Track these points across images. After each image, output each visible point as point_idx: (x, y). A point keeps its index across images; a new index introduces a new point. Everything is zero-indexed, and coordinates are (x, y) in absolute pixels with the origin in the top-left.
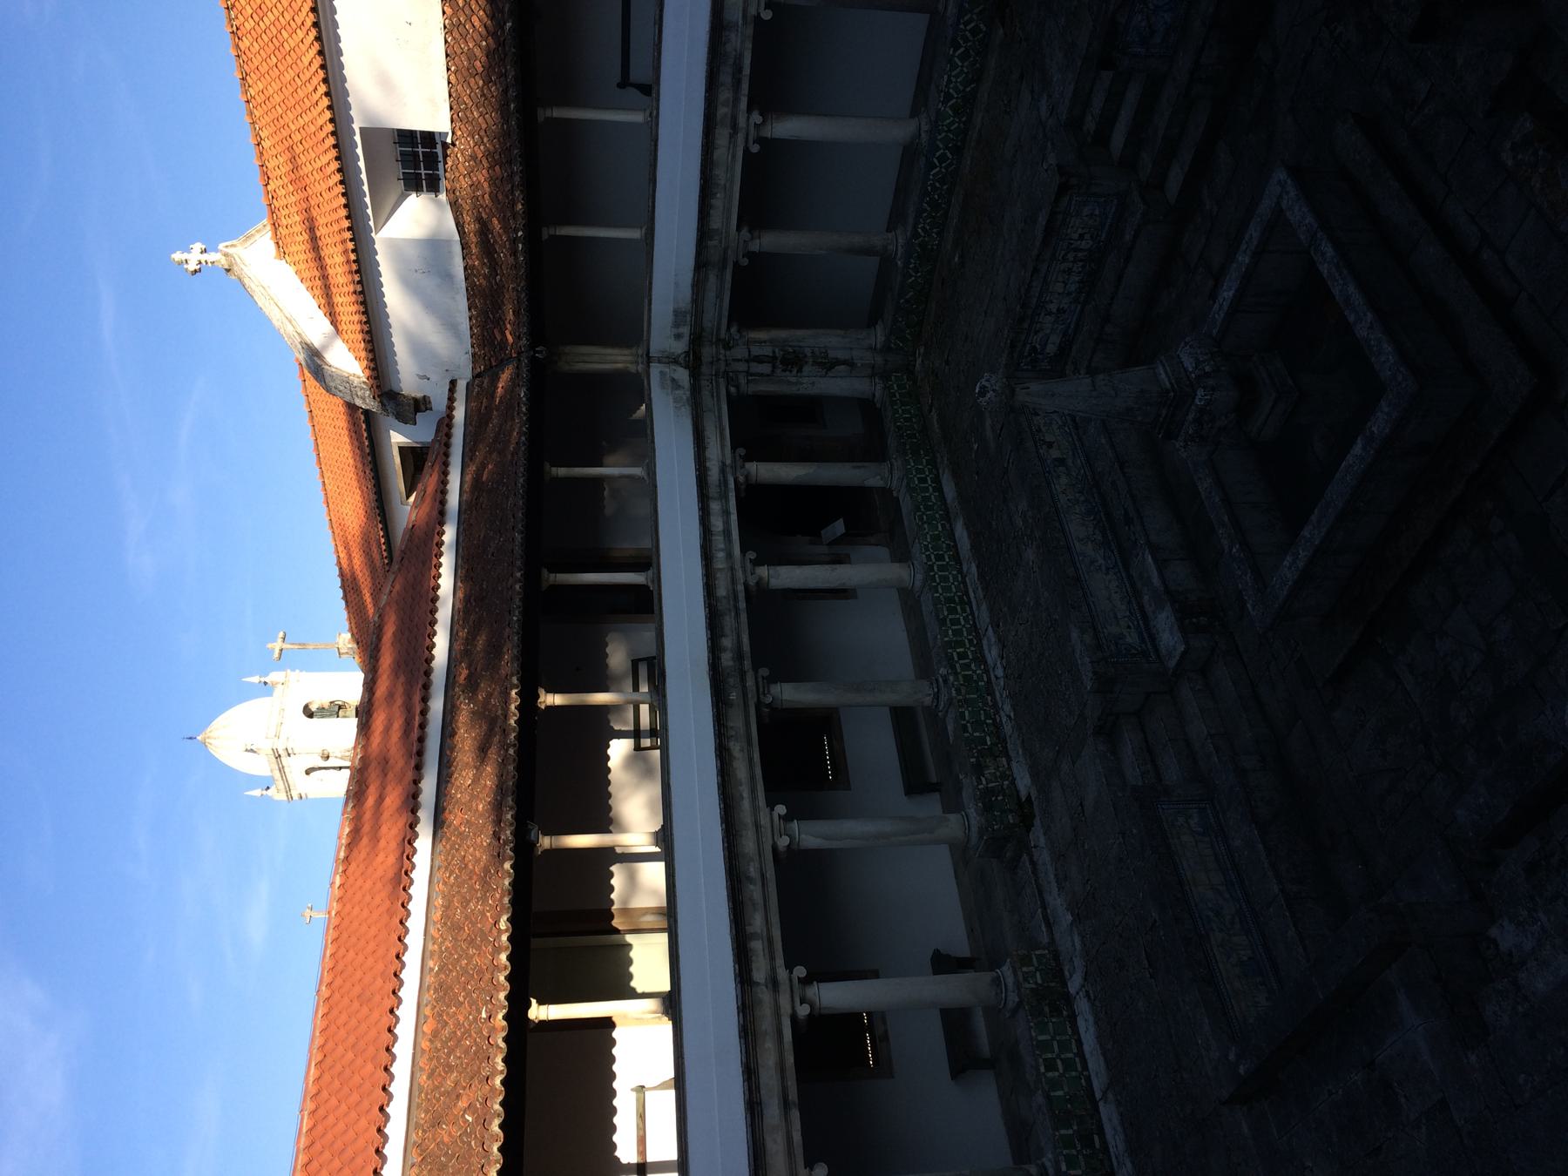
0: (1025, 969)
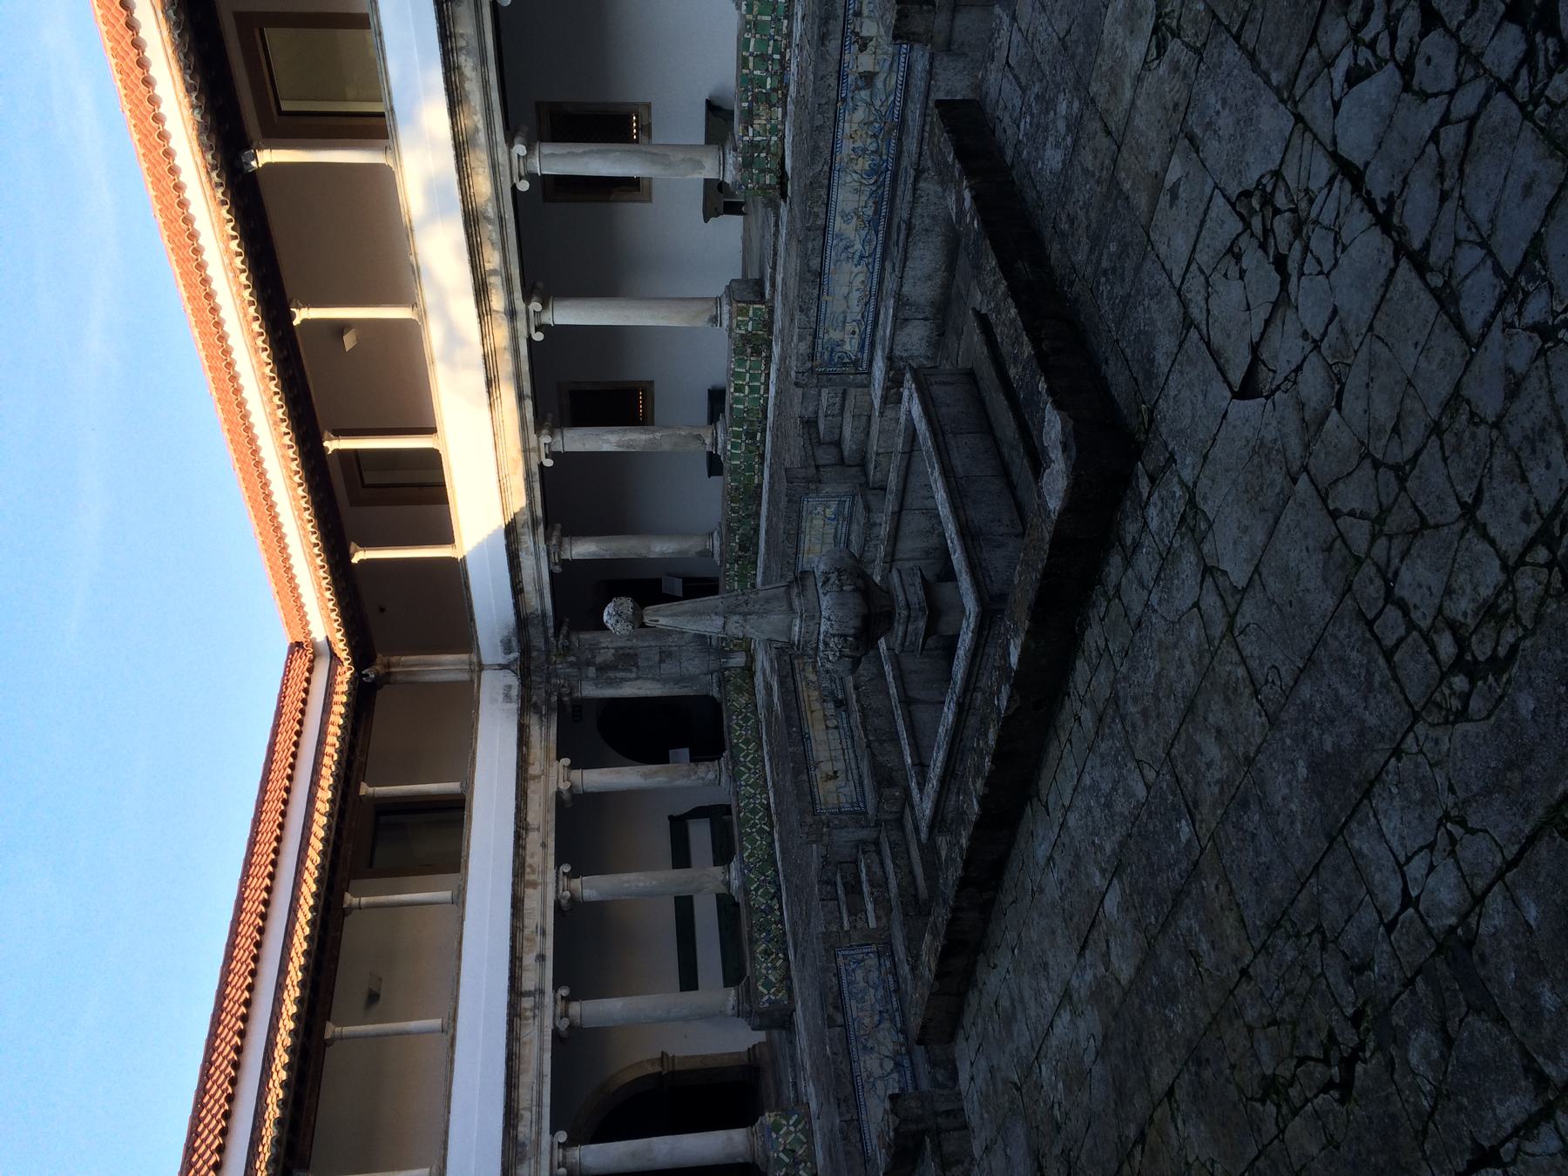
0: (739, 318)
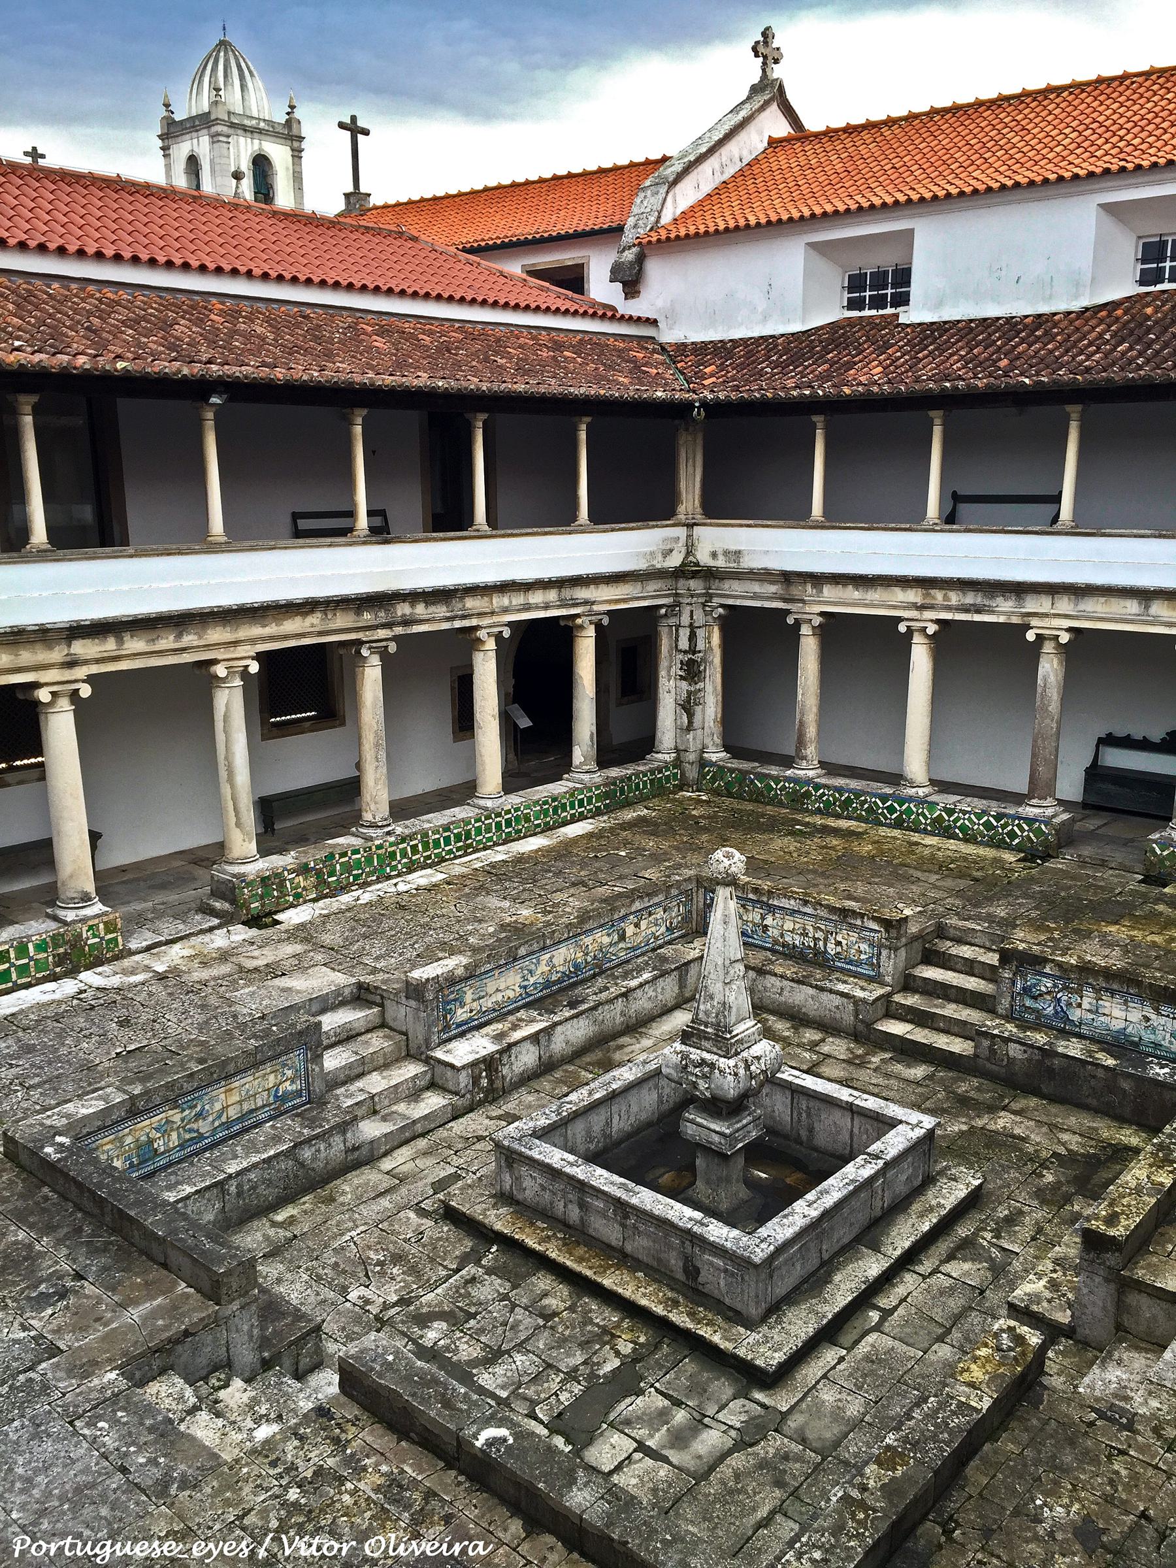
0: (101, 926)
